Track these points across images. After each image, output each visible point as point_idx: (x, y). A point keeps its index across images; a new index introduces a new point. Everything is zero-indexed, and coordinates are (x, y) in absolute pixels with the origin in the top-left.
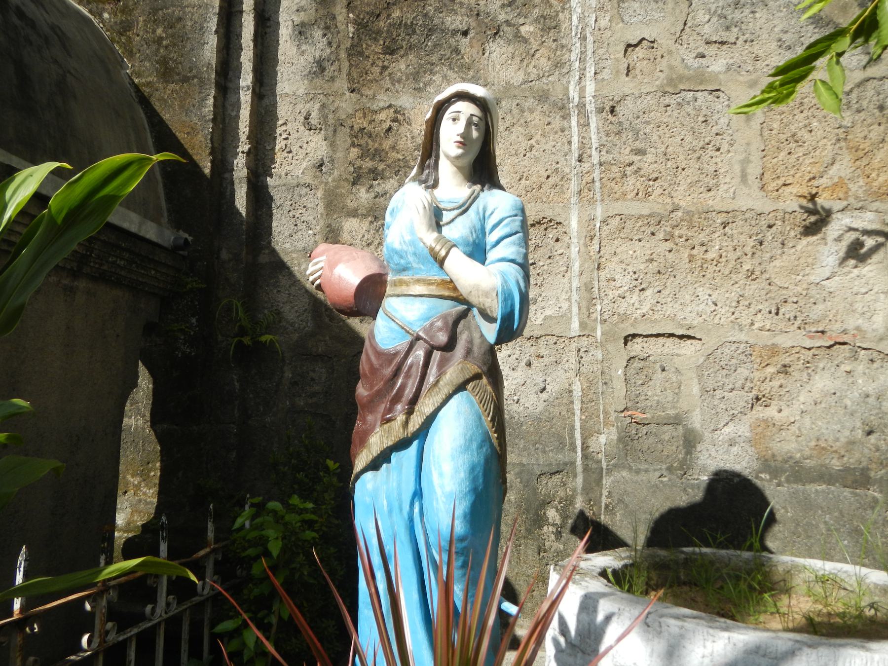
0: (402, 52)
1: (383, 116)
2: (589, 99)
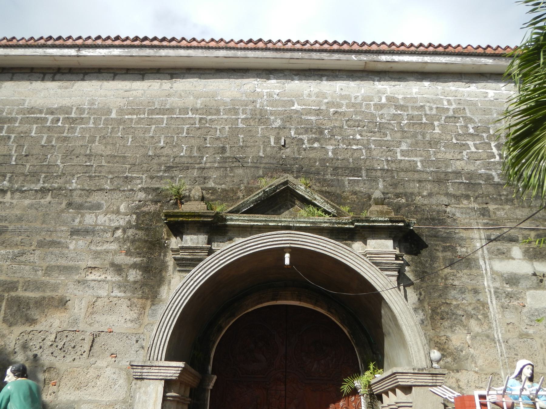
0: (445, 319)
1: (443, 338)
2: (500, 338)
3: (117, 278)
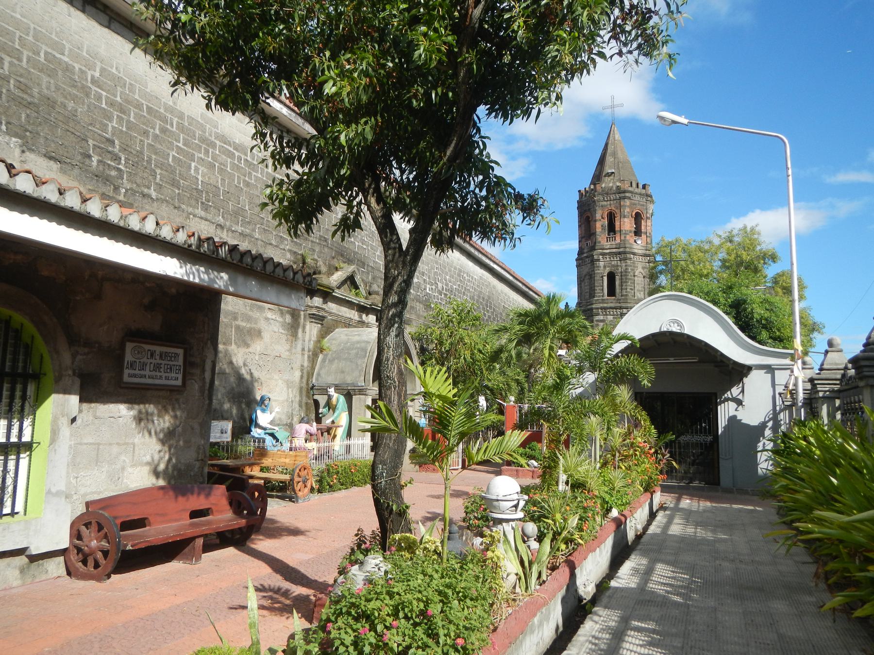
3: (281, 320)
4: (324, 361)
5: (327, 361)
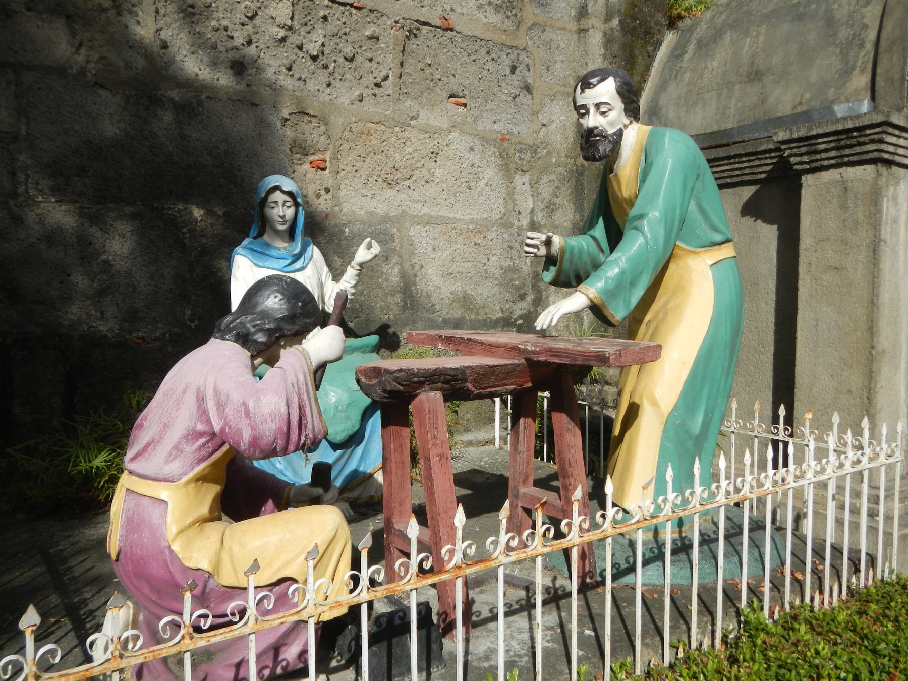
4: (677, 53)
5: (691, 48)
